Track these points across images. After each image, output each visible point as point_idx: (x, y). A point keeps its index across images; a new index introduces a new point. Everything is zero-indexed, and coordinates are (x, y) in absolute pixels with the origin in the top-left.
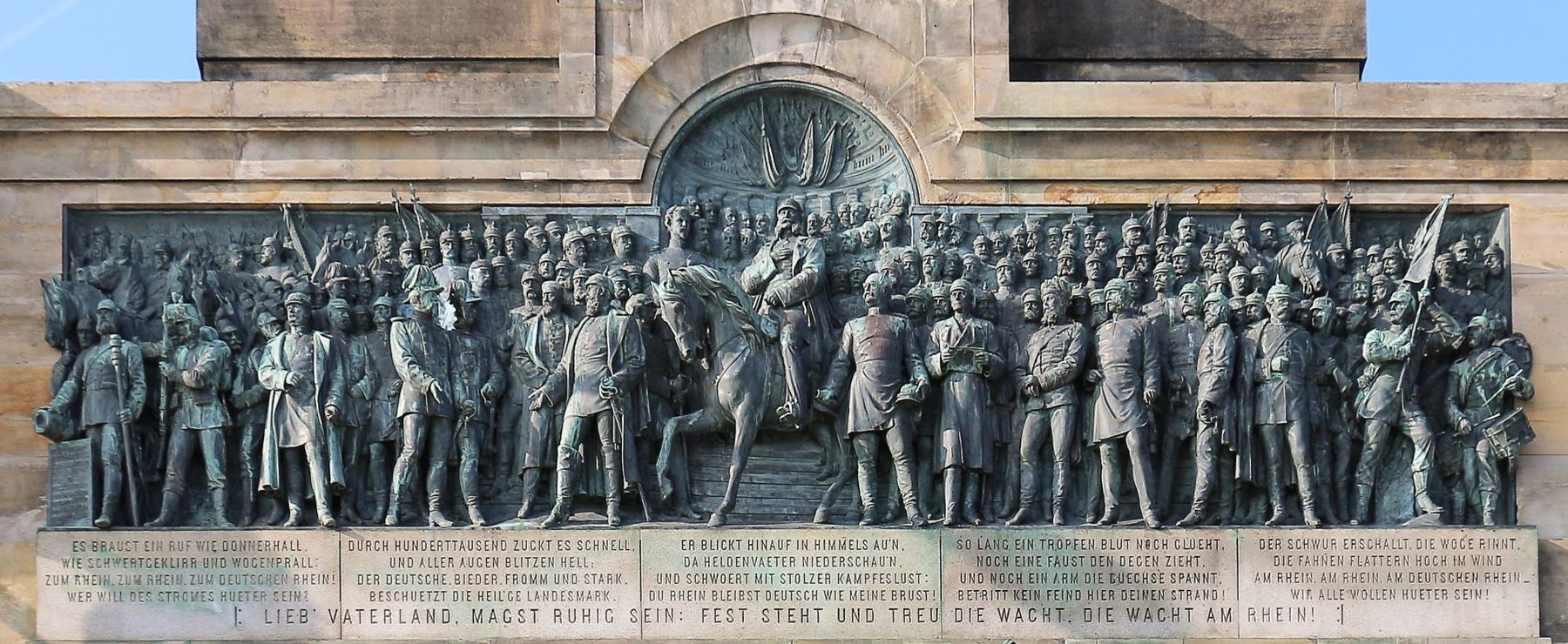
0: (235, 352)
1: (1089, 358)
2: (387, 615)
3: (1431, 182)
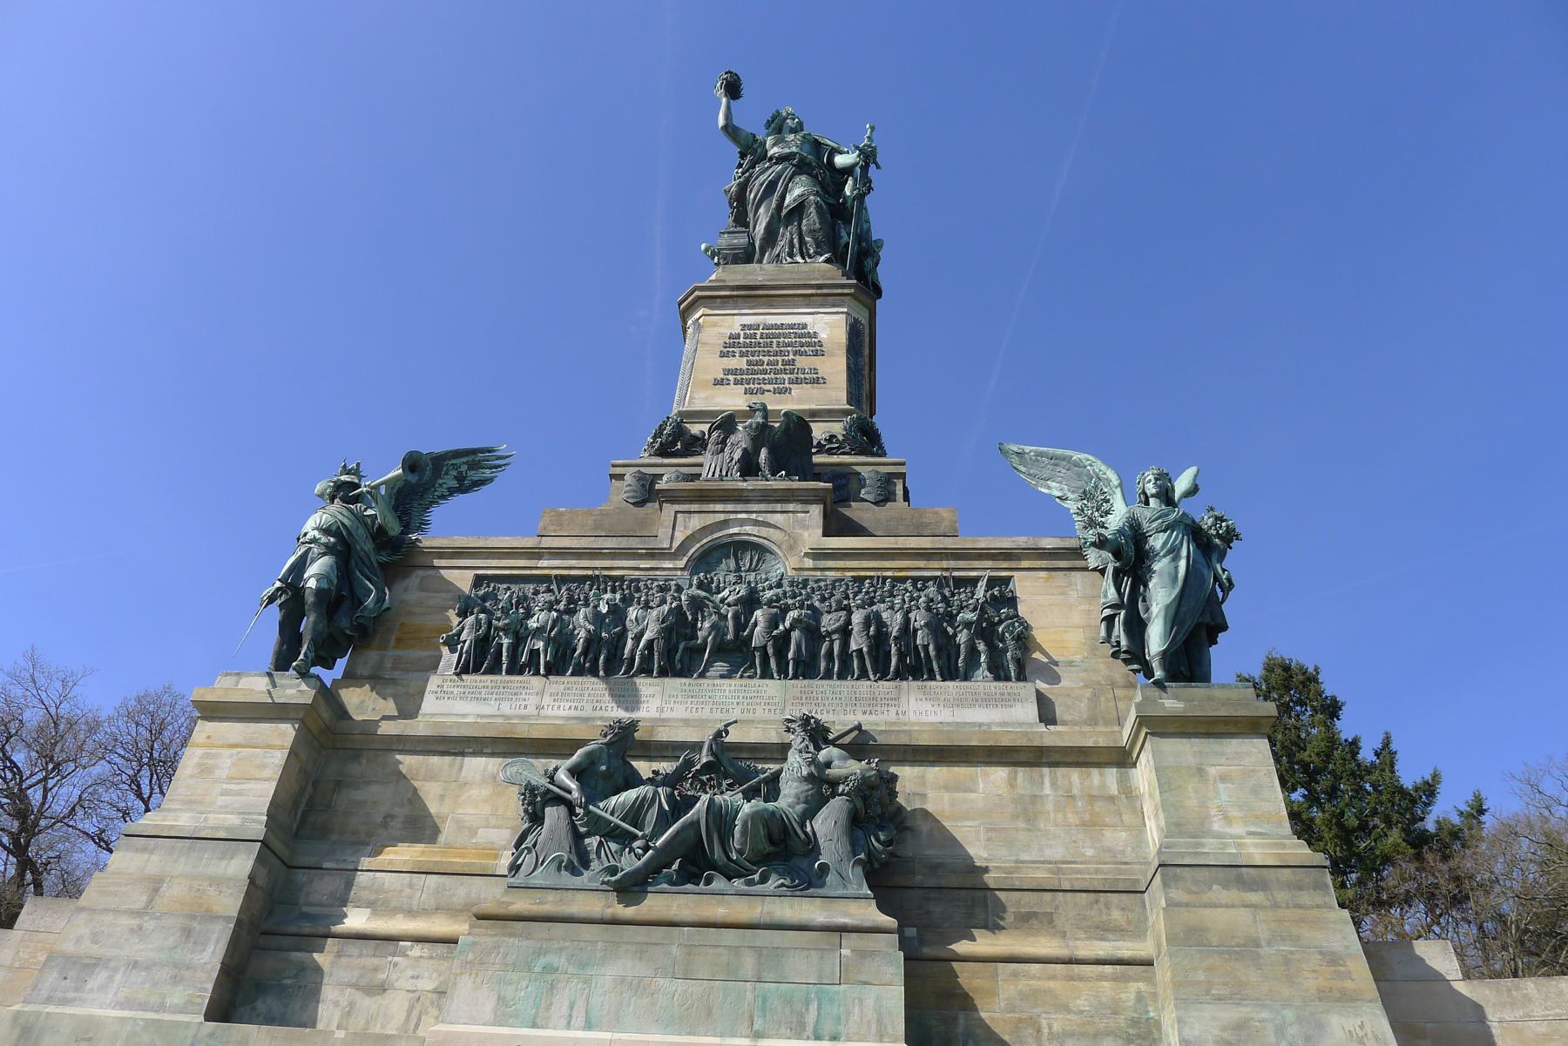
1: (848, 622)
3: (983, 570)
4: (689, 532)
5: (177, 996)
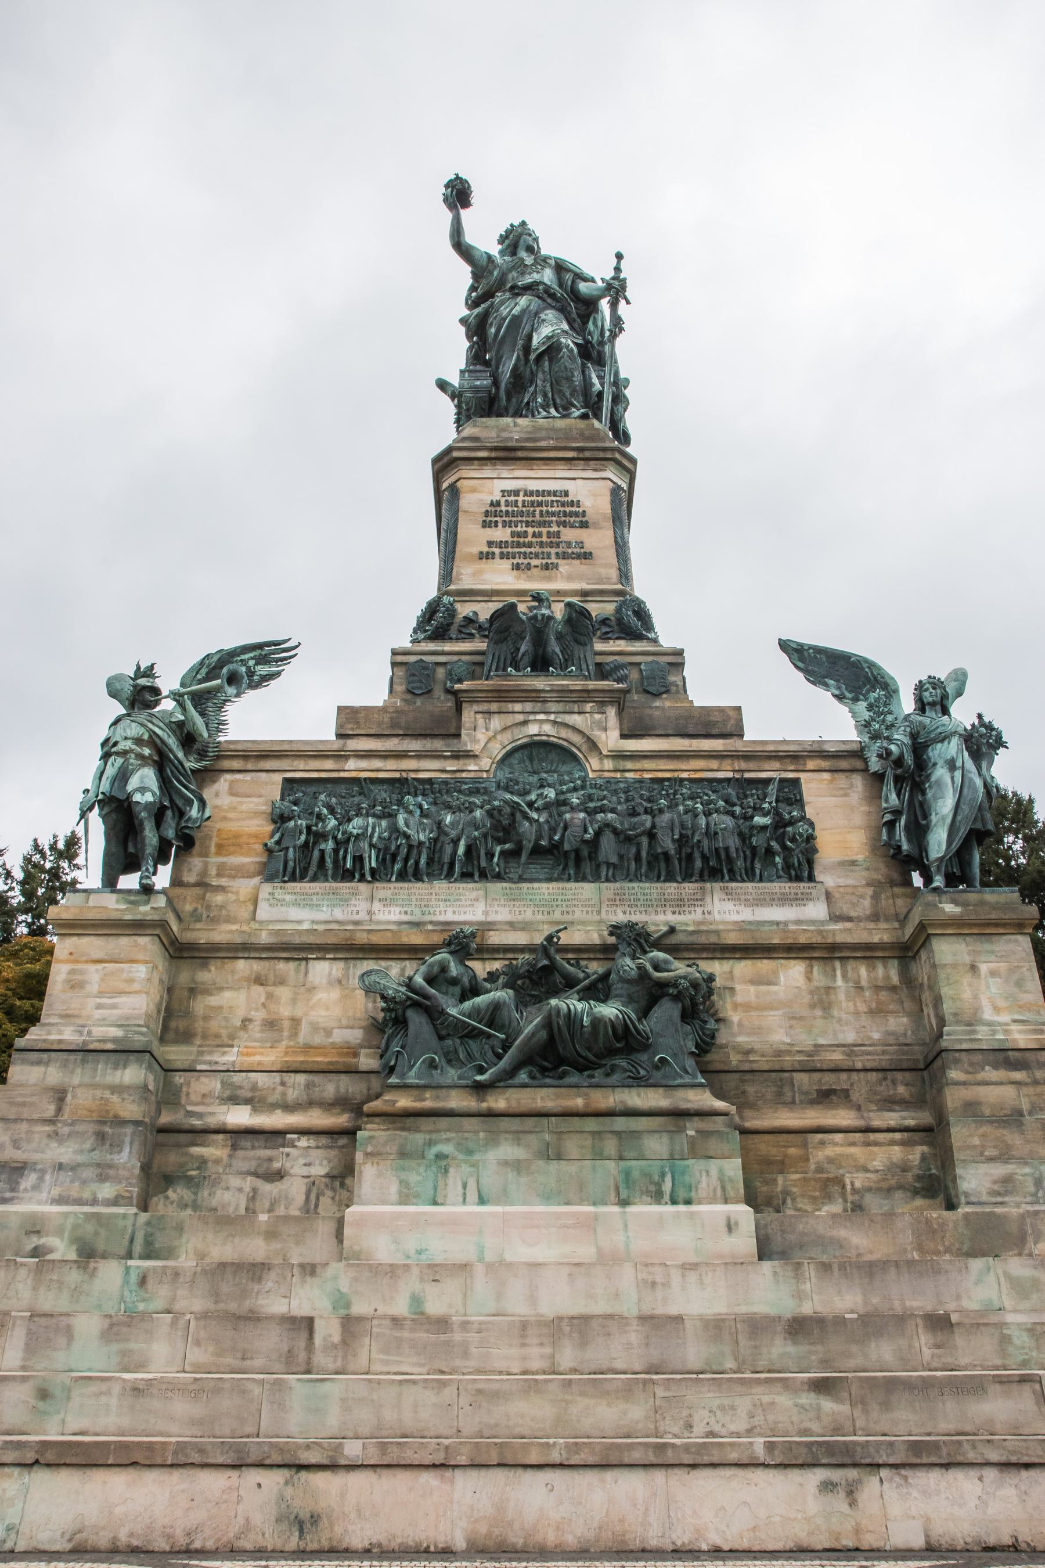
0: (340, 824)
2: (390, 912)
4: (491, 734)
5: (107, 1191)
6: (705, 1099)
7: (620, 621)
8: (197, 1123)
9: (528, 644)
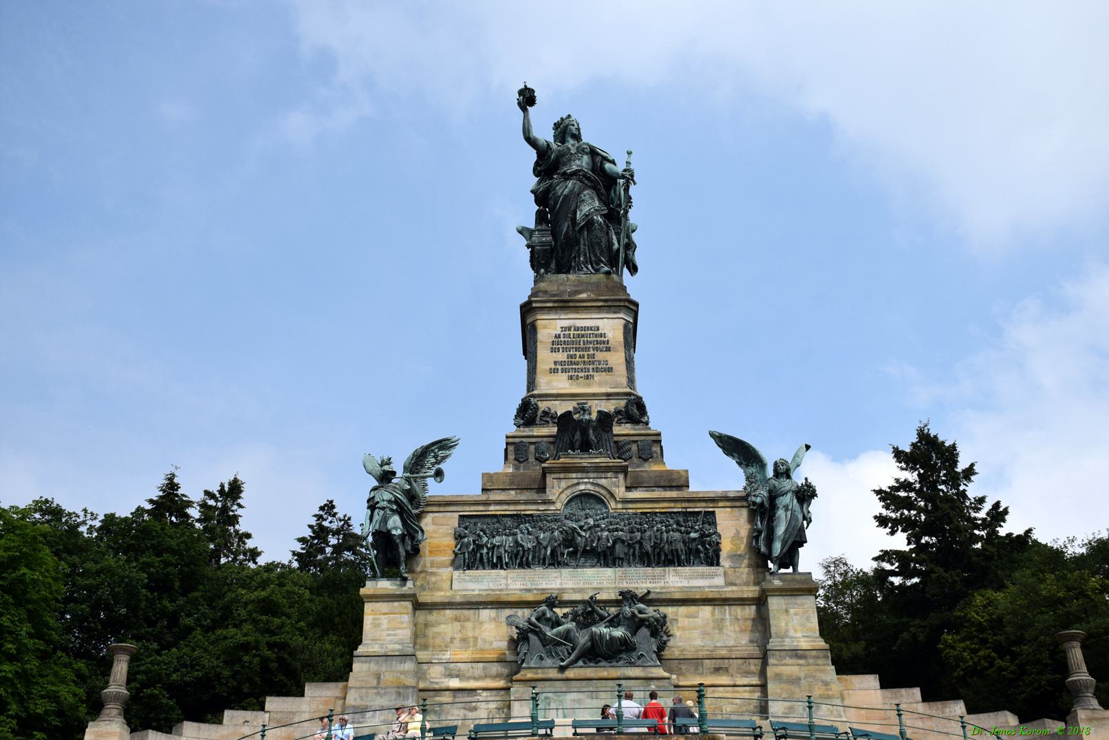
6: (660, 672)
7: (627, 411)
8: (437, 687)
9: (579, 433)
